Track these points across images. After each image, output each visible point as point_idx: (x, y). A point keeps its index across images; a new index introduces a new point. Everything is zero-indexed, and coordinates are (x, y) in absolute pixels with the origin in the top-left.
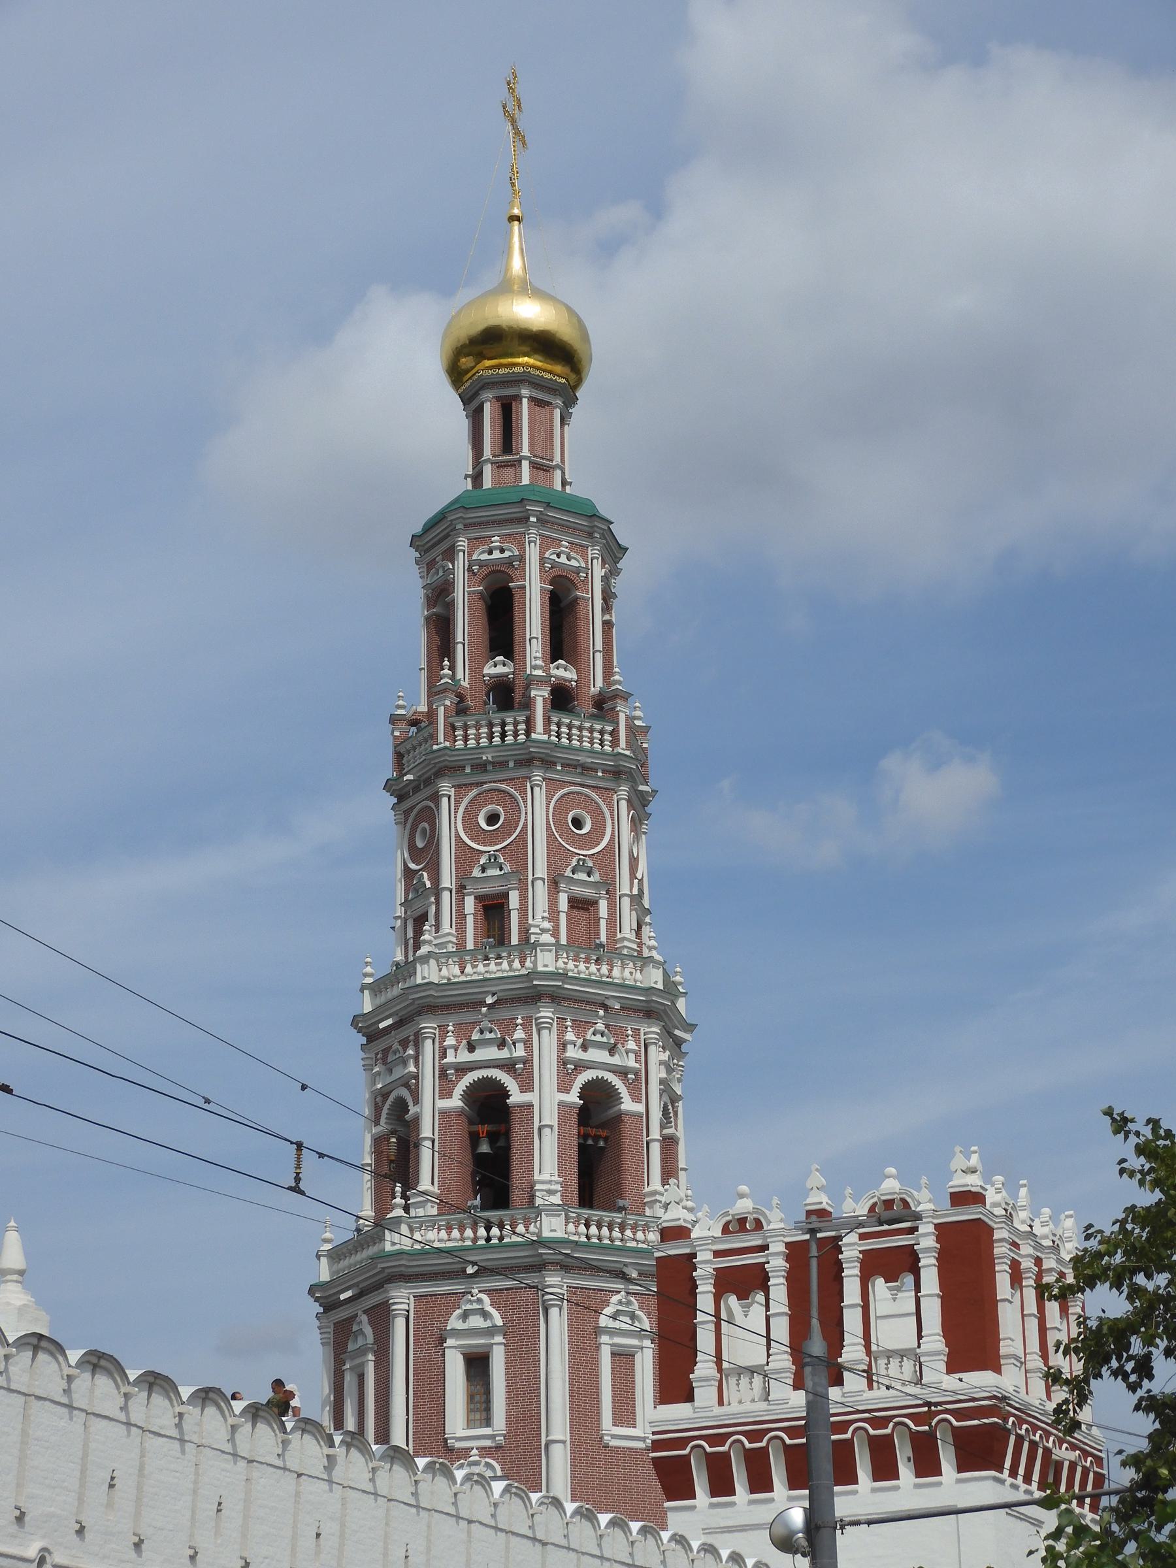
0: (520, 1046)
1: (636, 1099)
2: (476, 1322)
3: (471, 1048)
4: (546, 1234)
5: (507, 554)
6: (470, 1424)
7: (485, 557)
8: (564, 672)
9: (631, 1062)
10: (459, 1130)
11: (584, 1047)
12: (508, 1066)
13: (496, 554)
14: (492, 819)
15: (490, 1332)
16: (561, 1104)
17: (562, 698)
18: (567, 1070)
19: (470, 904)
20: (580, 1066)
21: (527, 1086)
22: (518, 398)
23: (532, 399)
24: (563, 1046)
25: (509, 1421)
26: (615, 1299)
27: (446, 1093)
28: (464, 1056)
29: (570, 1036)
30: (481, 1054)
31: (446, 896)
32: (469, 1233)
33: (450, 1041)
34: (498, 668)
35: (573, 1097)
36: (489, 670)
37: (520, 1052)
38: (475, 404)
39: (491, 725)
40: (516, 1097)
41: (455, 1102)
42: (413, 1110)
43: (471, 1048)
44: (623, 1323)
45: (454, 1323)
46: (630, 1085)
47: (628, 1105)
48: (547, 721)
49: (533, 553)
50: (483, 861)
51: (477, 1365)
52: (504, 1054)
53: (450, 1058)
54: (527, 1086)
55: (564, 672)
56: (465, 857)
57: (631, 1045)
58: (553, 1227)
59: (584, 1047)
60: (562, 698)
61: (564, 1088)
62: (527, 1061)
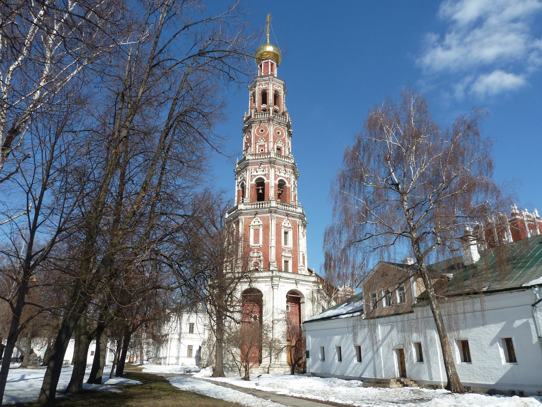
0: (267, 171)
1: (289, 184)
2: (257, 223)
4: (272, 205)
5: (266, 86)
6: (254, 243)
7: (262, 87)
8: (277, 108)
9: (289, 176)
10: (254, 189)
11: (280, 173)
15: (259, 225)
16: (275, 184)
17: (276, 111)
18: (276, 176)
19: (257, 147)
22: (268, 62)
25: (263, 243)
26: (285, 220)
27: (251, 181)
28: (255, 173)
29: (277, 170)
30: (259, 173)
31: (252, 145)
32: (256, 206)
33: (253, 171)
34: (264, 106)
35: (277, 182)
36: (262, 106)
37: (267, 172)
38: (260, 64)
39: (262, 114)
40: (266, 181)
41: (254, 182)
42: (245, 184)
43: (257, 172)
44: (286, 225)
45: (252, 223)
46: (288, 181)
47: (287, 185)
48: (273, 114)
50: (260, 139)
52: (264, 173)
53: (253, 174)
54: (268, 179)
55: (277, 108)
56: (257, 138)
57: (289, 173)
58: (274, 204)
59: (280, 173)
60: (276, 111)
61: (275, 179)
62: (269, 175)
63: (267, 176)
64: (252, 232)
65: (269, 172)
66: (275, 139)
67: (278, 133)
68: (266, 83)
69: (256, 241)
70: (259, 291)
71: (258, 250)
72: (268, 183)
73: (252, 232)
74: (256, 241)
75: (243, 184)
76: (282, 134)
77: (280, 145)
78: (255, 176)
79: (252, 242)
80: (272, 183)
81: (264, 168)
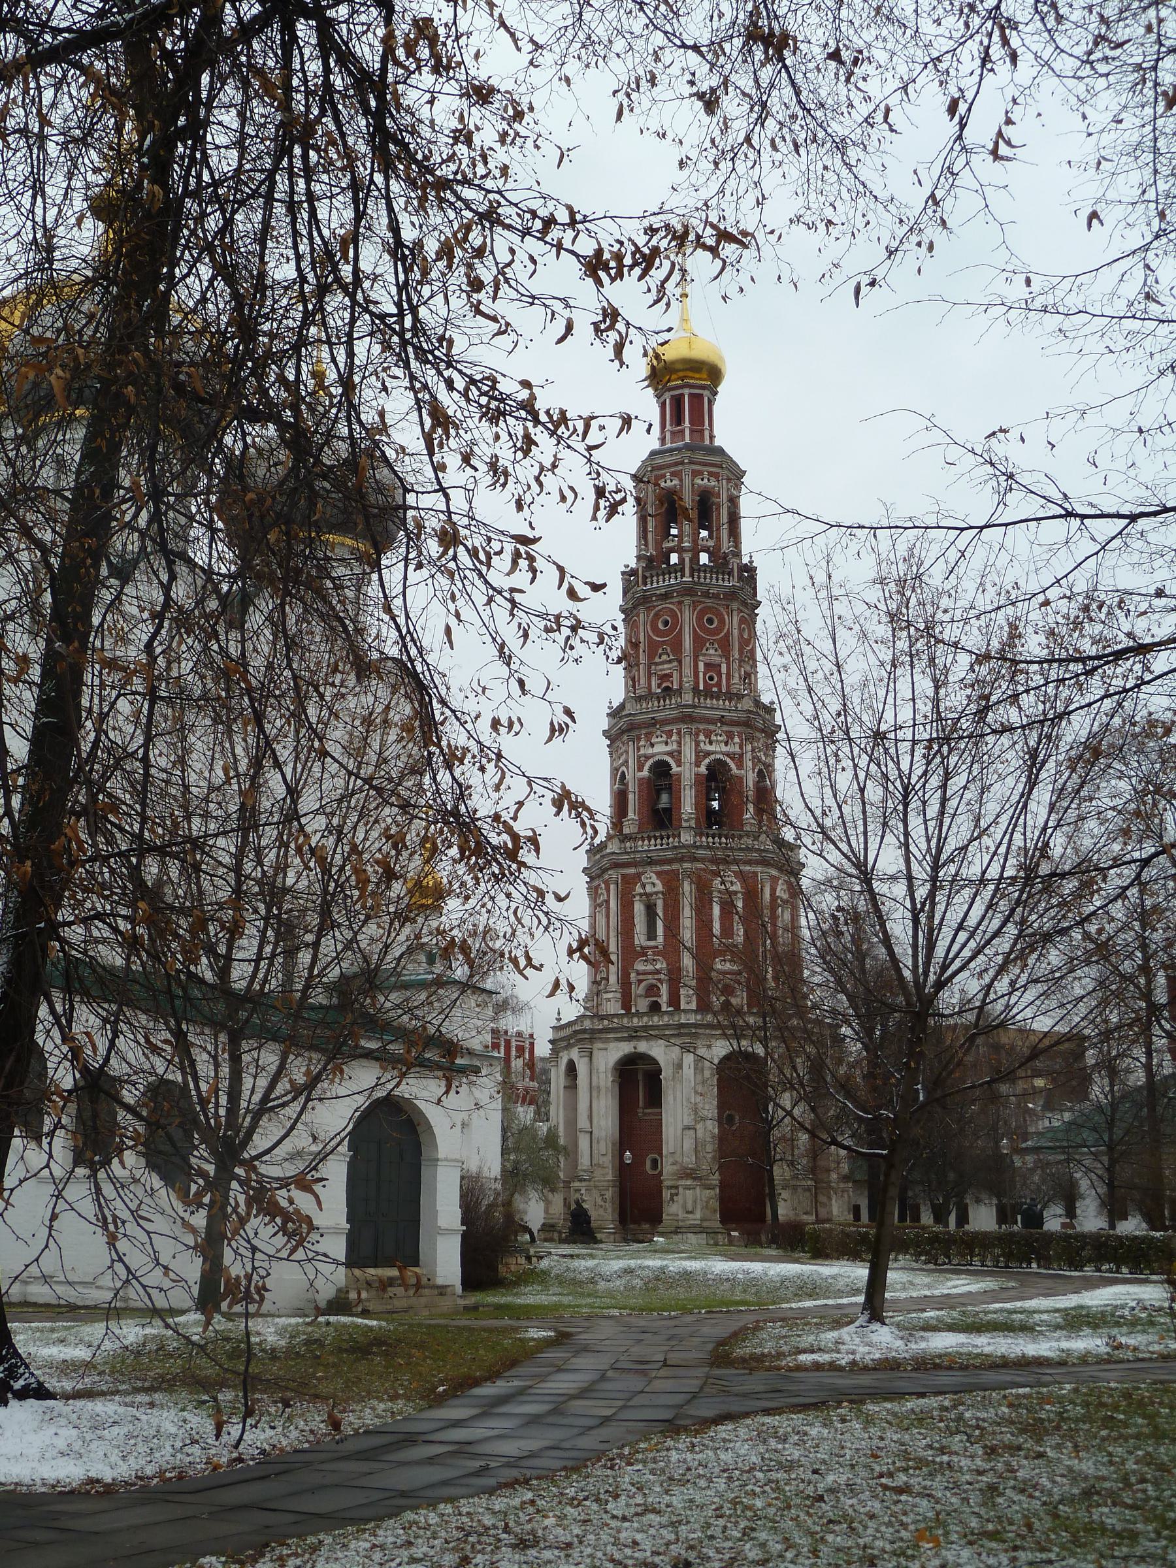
3: (652, 745)
9: (737, 749)
12: (670, 754)
13: (669, 484)
14: (666, 623)
15: (656, 893)
18: (700, 755)
20: (708, 754)
21: (679, 765)
23: (691, 395)
24: (697, 744)
27: (640, 769)
28: (650, 751)
29: (702, 737)
37: (675, 746)
40: (675, 769)
41: (645, 773)
45: (639, 889)
49: (687, 481)
51: (650, 910)
52: (668, 748)
57: (736, 740)
58: (686, 838)
62: (680, 752)
63: (677, 755)
64: (639, 908)
65: (679, 743)
66: (699, 644)
67: (710, 621)
68: (673, 474)
69: (652, 935)
70: (654, 1061)
71: (654, 954)
72: (679, 775)
73: (639, 908)
74: (651, 934)
75: (623, 775)
76: (722, 622)
77: (715, 660)
78: (647, 758)
79: (640, 939)
80: (687, 772)
81: (669, 734)
